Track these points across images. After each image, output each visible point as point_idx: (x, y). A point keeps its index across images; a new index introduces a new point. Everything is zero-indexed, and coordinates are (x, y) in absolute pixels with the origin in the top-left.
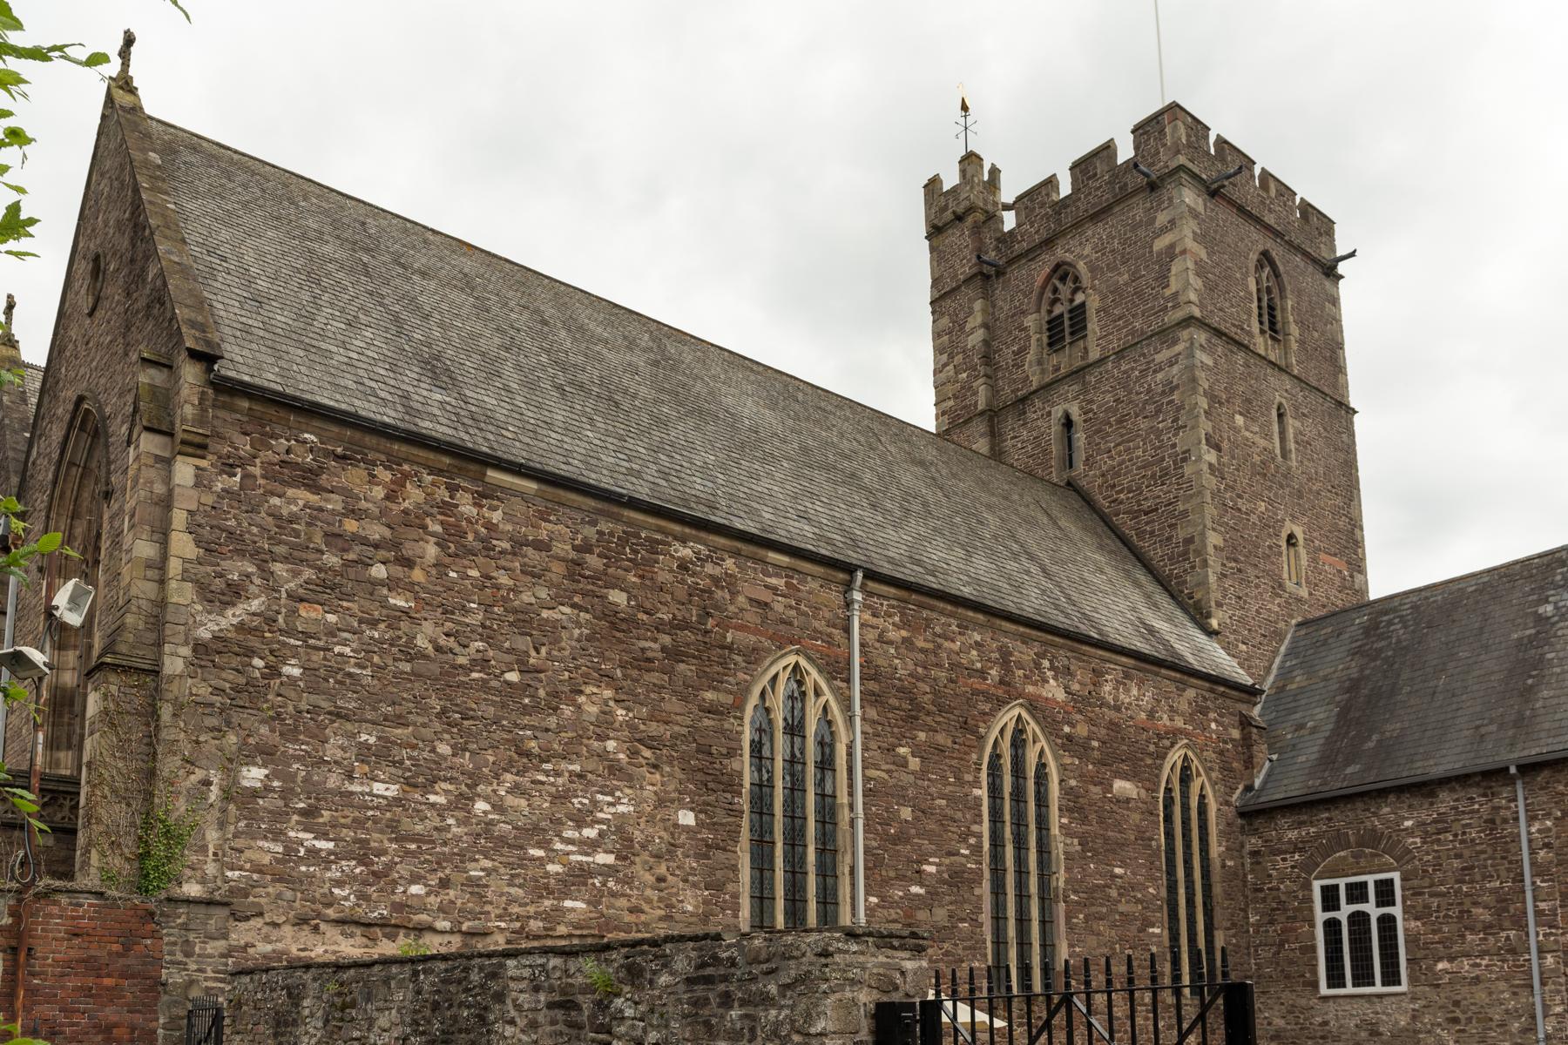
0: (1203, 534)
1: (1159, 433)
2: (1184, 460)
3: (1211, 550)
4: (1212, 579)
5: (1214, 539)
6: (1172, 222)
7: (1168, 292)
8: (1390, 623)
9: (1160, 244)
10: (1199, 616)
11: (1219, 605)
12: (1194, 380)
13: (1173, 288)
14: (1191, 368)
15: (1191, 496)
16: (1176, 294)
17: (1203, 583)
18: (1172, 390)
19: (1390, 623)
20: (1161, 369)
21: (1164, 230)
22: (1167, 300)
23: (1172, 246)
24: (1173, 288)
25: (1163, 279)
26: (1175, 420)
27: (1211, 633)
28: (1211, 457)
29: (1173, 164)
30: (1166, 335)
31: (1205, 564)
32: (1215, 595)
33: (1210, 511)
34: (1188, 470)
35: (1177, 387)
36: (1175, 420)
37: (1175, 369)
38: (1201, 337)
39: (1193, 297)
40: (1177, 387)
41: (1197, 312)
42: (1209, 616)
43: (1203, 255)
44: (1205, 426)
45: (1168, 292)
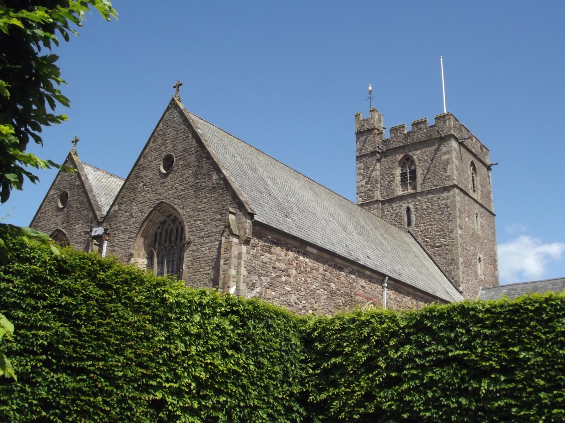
0: (458, 259)
1: (442, 221)
2: (451, 232)
3: (460, 264)
4: (461, 273)
5: (461, 260)
6: (448, 151)
7: (446, 174)
8: (514, 294)
9: (445, 157)
10: (456, 286)
11: (462, 282)
12: (455, 206)
13: (448, 173)
14: (454, 202)
15: (454, 245)
16: (449, 176)
17: (458, 275)
18: (448, 207)
19: (514, 294)
20: (444, 199)
21: (445, 153)
22: (446, 177)
23: (448, 159)
24: (448, 173)
25: (445, 170)
26: (449, 218)
27: (461, 293)
28: (460, 232)
29: (449, 133)
30: (446, 189)
31: (458, 268)
32: (461, 279)
33: (460, 250)
34: (453, 235)
35: (449, 207)
36: (449, 218)
37: (449, 201)
38: (457, 191)
39: (455, 178)
40: (449, 207)
41: (456, 183)
42: (459, 286)
43: (458, 164)
44: (458, 221)
45: (446, 174)
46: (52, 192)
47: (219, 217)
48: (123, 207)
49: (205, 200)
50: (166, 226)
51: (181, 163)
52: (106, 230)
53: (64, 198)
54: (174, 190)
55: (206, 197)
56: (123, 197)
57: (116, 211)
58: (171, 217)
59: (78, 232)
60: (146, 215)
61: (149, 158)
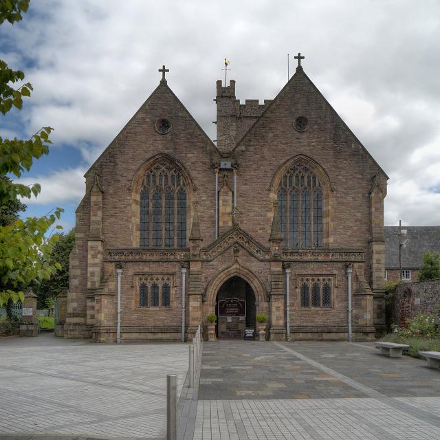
46: (141, 115)
47: (360, 176)
48: (251, 149)
49: (345, 162)
50: (297, 172)
51: (316, 127)
52: (236, 166)
53: (164, 124)
54: (311, 148)
55: (346, 160)
56: (250, 141)
57: (243, 151)
58: (302, 167)
59: (193, 160)
60: (282, 162)
61: (278, 114)
